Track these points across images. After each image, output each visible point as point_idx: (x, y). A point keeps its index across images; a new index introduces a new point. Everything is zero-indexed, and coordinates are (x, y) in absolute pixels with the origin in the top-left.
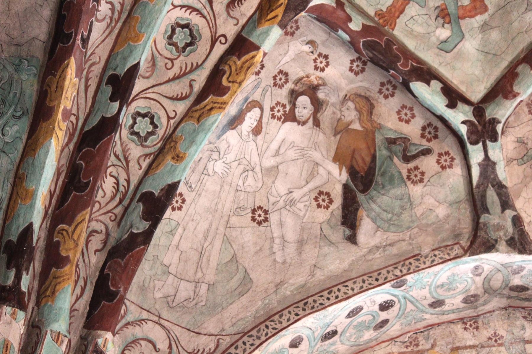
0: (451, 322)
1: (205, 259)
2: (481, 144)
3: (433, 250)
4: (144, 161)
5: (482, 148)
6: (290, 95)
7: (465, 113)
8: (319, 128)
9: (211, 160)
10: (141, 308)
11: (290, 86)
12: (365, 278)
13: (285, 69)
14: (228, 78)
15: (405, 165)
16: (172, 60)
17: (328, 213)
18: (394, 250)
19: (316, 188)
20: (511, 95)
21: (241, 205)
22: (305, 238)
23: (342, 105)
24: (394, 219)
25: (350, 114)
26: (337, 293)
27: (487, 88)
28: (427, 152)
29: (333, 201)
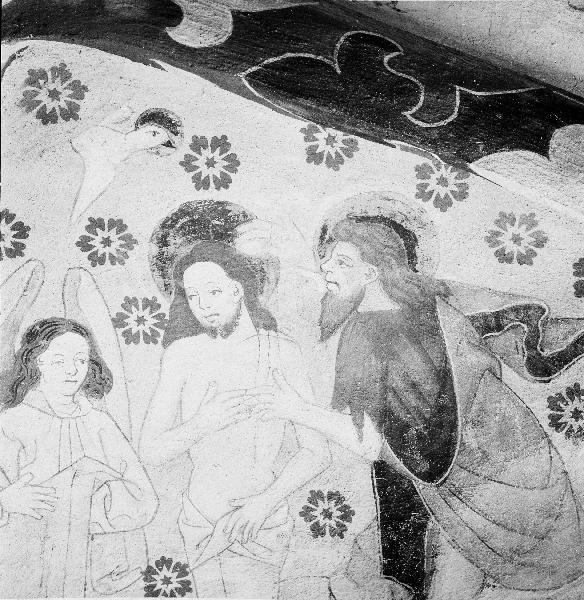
6: (157, 273)
19: (300, 489)
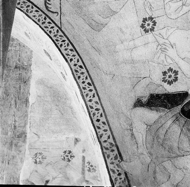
3: (126, 174)
12: (101, 111)
19: (179, 68)
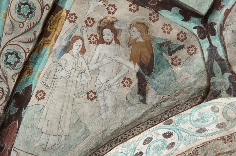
0: (216, 140)
1: (62, 123)
2: (207, 38)
4: (16, 77)
5: (208, 40)
7: (195, 22)
8: (119, 44)
9: (57, 70)
10: (27, 153)
11: (96, 25)
13: (91, 16)
14: (50, 27)
15: (170, 57)
16: (22, 23)
17: (130, 89)
18: (165, 104)
20: (220, 7)
21: (80, 92)
22: (118, 104)
23: (130, 30)
24: (166, 87)
25: (136, 34)
26: (134, 132)
27: (210, 5)
28: (181, 47)
29: (132, 82)
